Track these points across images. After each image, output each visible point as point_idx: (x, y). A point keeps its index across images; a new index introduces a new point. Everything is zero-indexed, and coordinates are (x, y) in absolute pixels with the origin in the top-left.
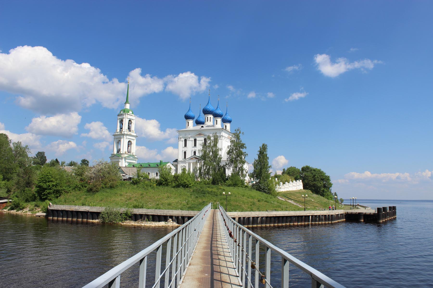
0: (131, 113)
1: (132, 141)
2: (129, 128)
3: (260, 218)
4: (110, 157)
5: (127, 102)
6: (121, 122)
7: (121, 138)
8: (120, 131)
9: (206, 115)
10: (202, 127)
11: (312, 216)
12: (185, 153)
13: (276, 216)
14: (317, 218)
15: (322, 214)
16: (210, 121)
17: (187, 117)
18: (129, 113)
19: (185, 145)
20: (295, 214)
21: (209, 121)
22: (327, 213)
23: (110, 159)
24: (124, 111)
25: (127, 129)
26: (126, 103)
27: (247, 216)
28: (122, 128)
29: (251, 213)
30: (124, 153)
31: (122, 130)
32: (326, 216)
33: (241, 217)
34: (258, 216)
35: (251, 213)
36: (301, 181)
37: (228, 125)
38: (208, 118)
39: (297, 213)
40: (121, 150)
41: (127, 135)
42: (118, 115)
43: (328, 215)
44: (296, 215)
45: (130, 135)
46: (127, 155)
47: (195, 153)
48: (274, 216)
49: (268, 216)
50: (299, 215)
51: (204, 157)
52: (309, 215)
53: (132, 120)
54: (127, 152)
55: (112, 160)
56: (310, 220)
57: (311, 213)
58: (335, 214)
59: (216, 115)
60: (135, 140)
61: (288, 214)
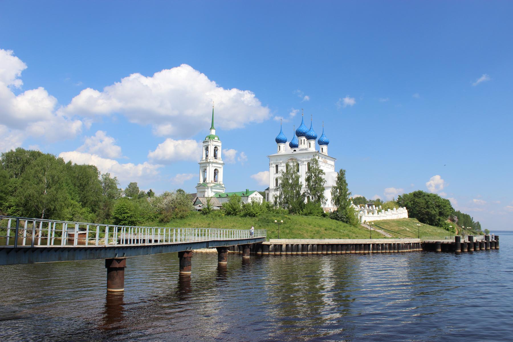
0: (217, 139)
1: (218, 169)
2: (215, 156)
3: (310, 245)
4: (196, 187)
5: (212, 127)
6: (207, 149)
7: (206, 166)
8: (206, 159)
10: (295, 151)
11: (373, 244)
14: (380, 246)
15: (386, 243)
17: (279, 141)
18: (214, 139)
21: (303, 143)
23: (196, 189)
24: (209, 138)
25: (213, 155)
26: (211, 129)
27: (296, 244)
28: (208, 156)
30: (210, 182)
31: (208, 158)
35: (301, 241)
37: (325, 147)
38: (301, 140)
40: (207, 179)
41: (213, 163)
42: (203, 142)
43: (394, 244)
44: (353, 243)
45: (216, 163)
46: (214, 184)
49: (319, 243)
51: (285, 185)
52: (369, 243)
53: (218, 147)
54: (213, 181)
55: (198, 190)
59: (309, 138)
60: (222, 168)
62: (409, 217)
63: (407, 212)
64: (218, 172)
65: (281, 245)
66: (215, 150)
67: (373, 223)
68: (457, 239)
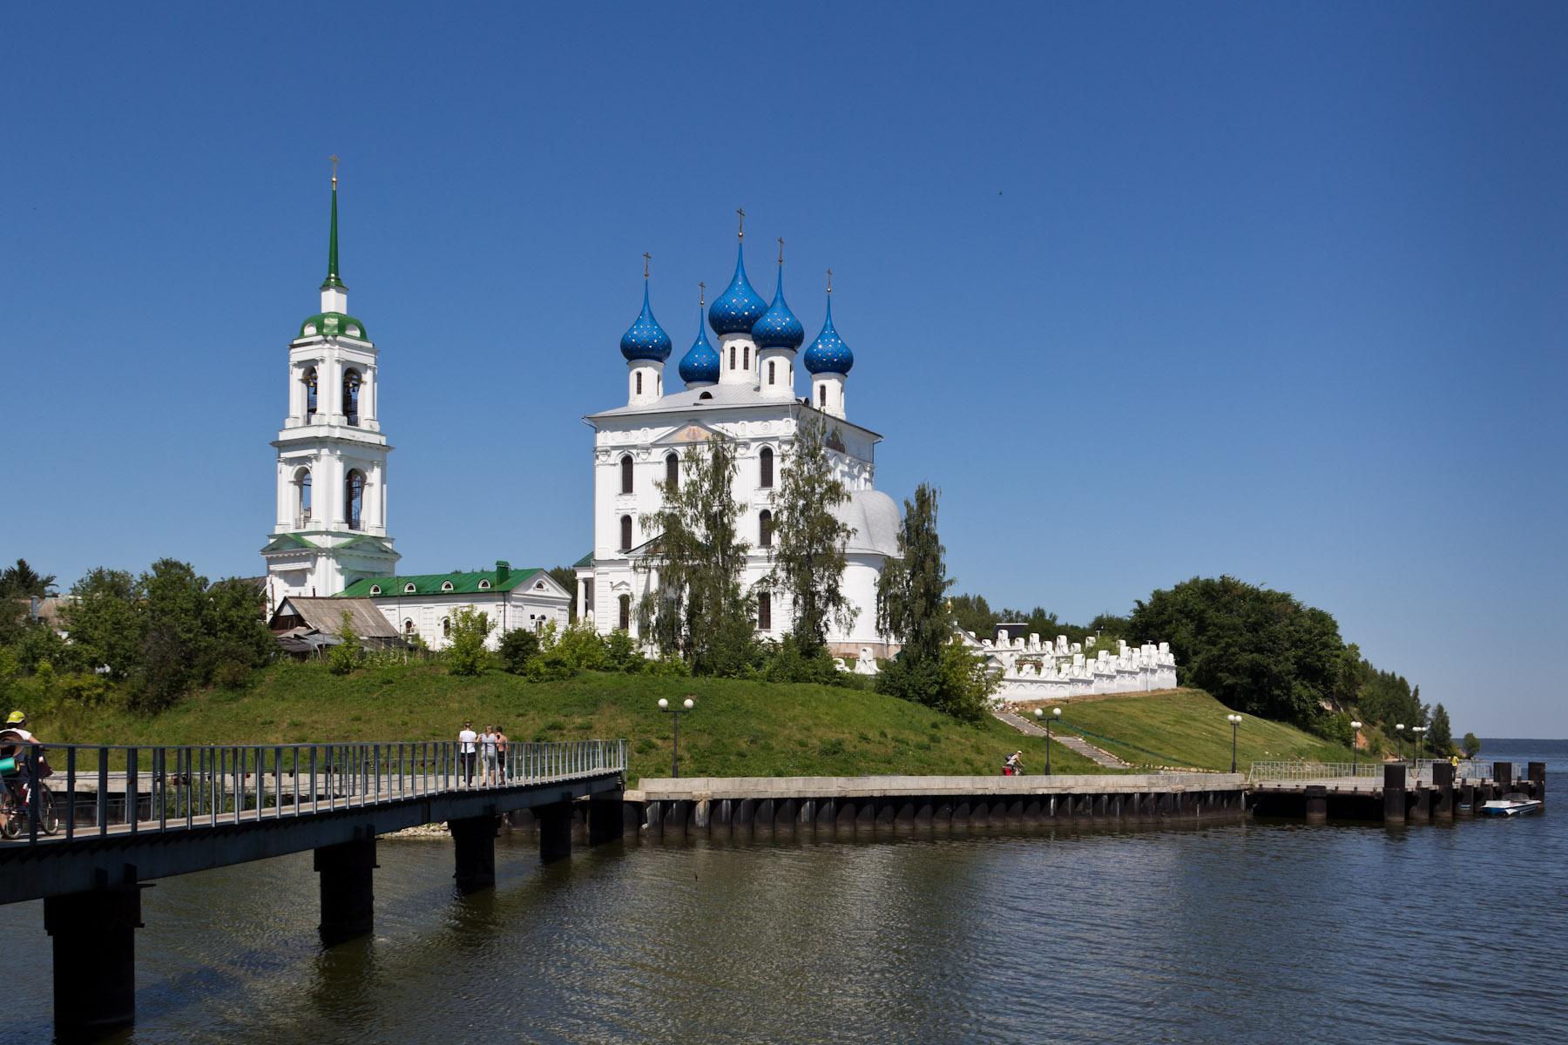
9: (724, 336)
10: (706, 396)
13: (885, 796)
15: (1111, 790)
16: (746, 367)
17: (635, 352)
19: (627, 486)
22: (1139, 784)
32: (1133, 801)
48: (875, 795)
50: (997, 793)
52: (1045, 791)
59: (769, 342)
64: (363, 481)
66: (345, 386)
67: (1057, 711)
68: (1394, 776)
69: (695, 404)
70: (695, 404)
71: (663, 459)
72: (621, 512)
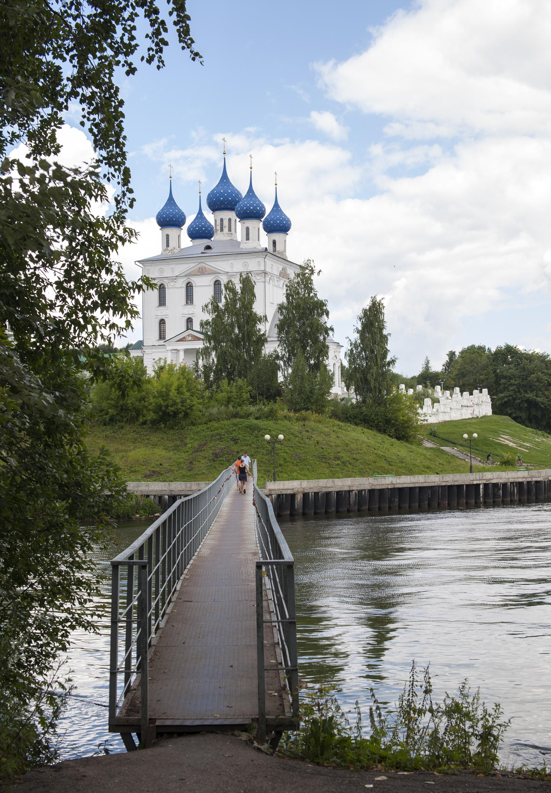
11: (486, 485)
12: (162, 322)
13: (394, 488)
15: (511, 480)
20: (441, 480)
21: (226, 230)
22: (526, 476)
29: (333, 482)
33: (309, 493)
34: (351, 489)
35: (333, 482)
36: (485, 391)
39: (447, 480)
43: (529, 483)
44: (444, 484)
47: (189, 321)
48: (389, 487)
49: (373, 487)
50: (453, 484)
52: (478, 482)
56: (481, 495)
57: (484, 478)
58: (546, 480)
61: (423, 481)
62: (494, 413)
63: (490, 400)
65: (293, 496)
69: (202, 253)
70: (202, 253)
71: (184, 285)
72: (159, 317)
